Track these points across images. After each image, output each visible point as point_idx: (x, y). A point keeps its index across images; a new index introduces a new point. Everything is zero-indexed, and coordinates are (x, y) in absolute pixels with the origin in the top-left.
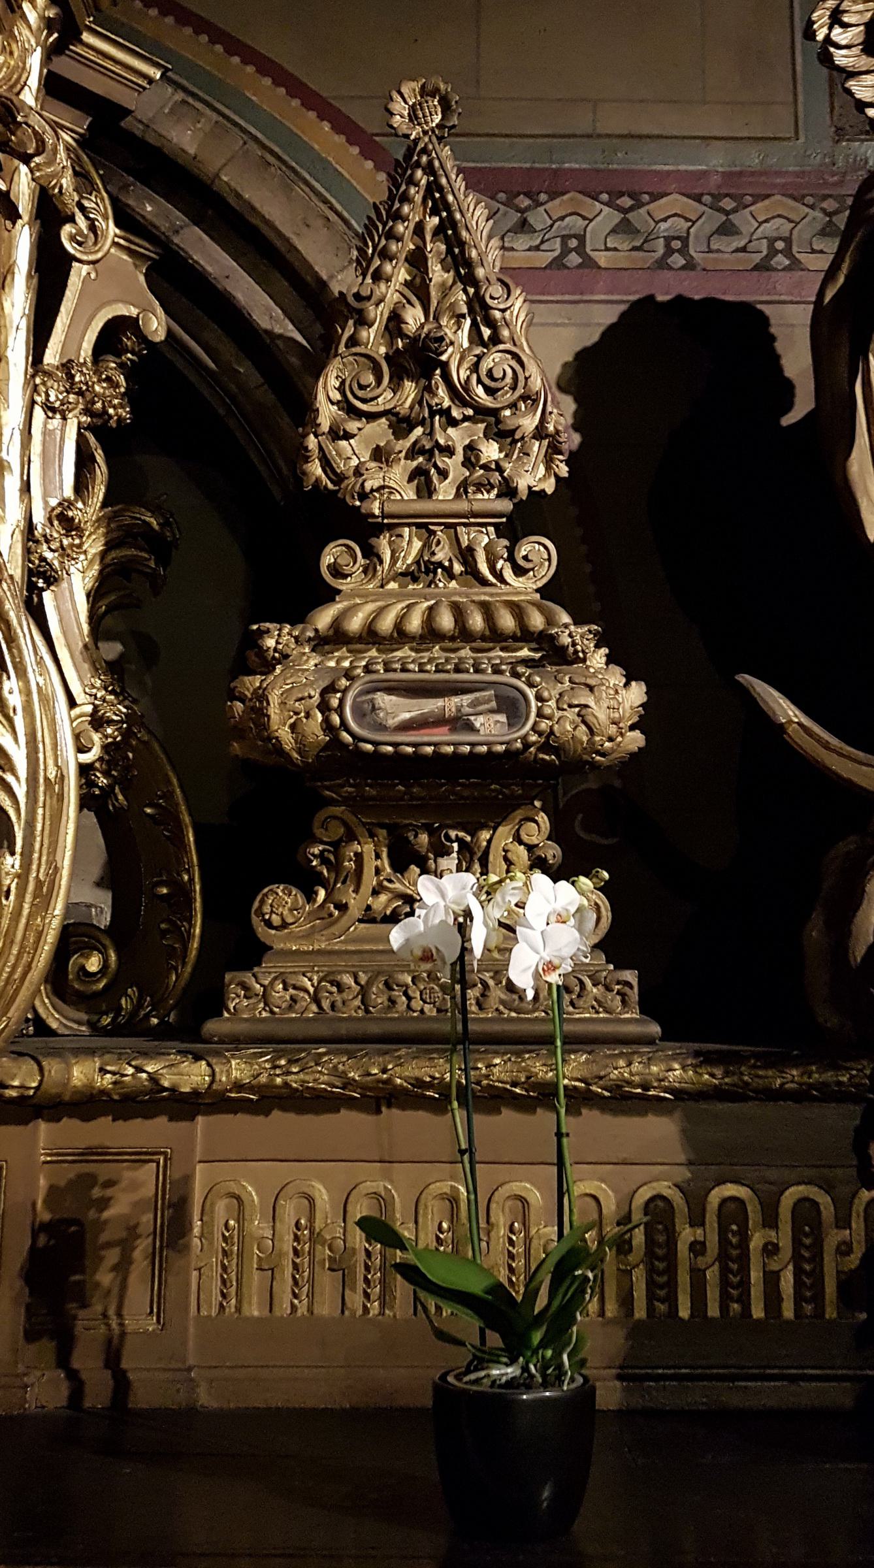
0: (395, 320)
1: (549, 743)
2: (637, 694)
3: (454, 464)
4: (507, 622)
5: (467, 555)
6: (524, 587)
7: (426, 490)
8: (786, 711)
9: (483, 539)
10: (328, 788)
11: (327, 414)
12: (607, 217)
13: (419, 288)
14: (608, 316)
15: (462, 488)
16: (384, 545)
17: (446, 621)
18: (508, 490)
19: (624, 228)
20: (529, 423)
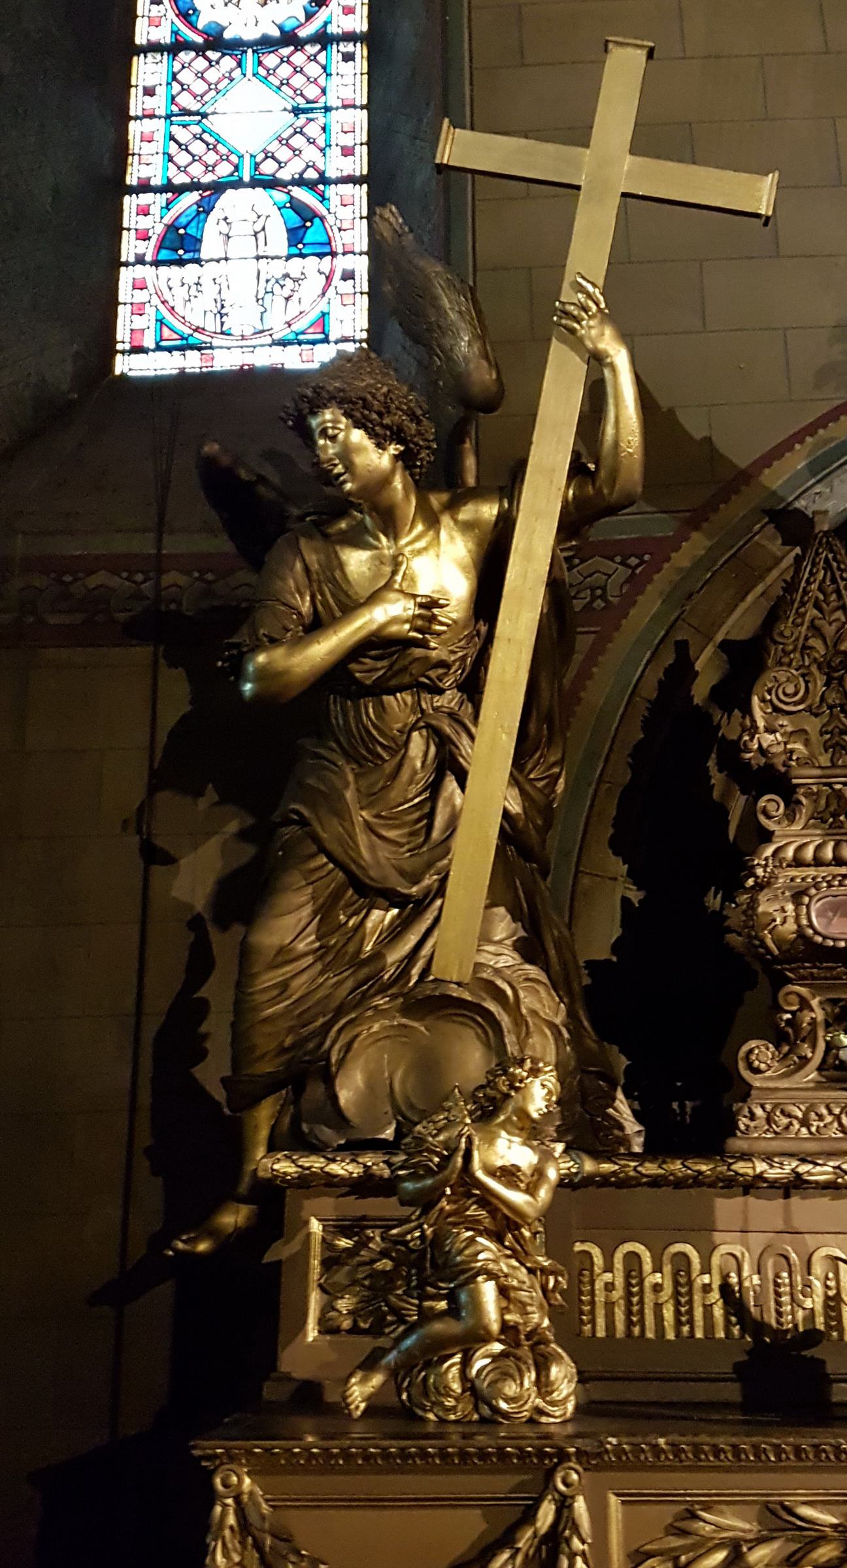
10: (790, 970)
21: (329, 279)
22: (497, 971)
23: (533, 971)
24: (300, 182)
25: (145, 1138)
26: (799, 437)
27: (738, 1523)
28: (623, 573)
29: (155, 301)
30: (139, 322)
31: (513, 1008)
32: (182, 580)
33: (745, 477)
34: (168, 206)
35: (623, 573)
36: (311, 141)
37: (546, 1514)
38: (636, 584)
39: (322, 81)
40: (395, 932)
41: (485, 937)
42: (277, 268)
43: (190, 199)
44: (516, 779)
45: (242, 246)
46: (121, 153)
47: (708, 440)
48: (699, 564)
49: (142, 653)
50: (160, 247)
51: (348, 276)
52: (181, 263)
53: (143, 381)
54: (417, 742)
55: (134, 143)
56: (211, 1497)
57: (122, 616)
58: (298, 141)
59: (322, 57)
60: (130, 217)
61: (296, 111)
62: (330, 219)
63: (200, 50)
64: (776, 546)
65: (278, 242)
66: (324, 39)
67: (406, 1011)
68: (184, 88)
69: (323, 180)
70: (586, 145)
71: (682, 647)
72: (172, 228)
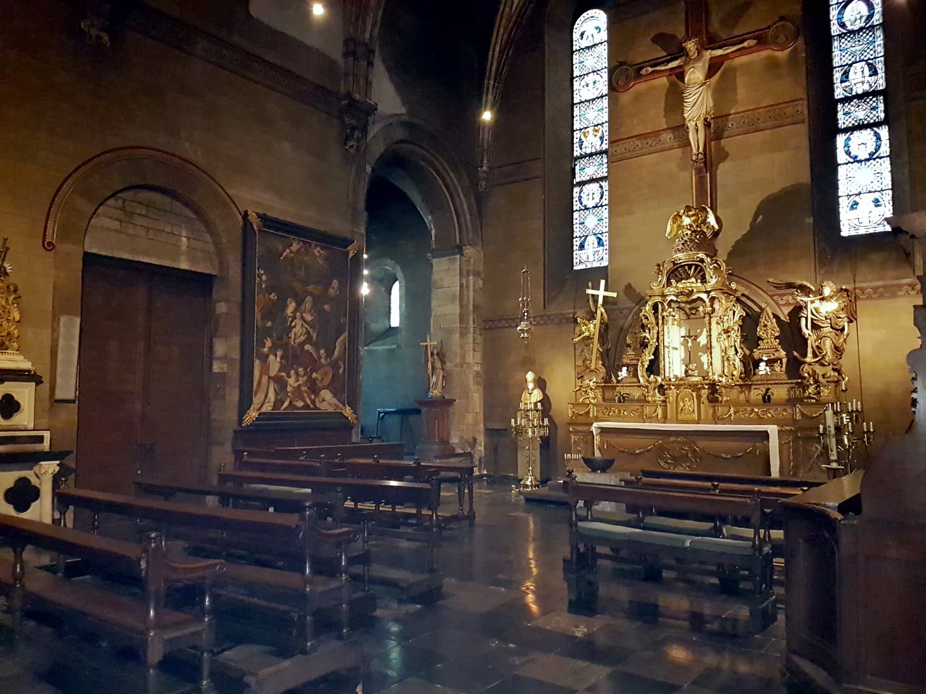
6: (776, 344)
9: (773, 340)
11: (758, 330)
12: (791, 298)
13: (766, 319)
42: (595, 250)
43: (583, 238)
45: (591, 246)
55: (575, 230)
60: (575, 243)
63: (583, 210)
66: (602, 206)
72: (581, 244)
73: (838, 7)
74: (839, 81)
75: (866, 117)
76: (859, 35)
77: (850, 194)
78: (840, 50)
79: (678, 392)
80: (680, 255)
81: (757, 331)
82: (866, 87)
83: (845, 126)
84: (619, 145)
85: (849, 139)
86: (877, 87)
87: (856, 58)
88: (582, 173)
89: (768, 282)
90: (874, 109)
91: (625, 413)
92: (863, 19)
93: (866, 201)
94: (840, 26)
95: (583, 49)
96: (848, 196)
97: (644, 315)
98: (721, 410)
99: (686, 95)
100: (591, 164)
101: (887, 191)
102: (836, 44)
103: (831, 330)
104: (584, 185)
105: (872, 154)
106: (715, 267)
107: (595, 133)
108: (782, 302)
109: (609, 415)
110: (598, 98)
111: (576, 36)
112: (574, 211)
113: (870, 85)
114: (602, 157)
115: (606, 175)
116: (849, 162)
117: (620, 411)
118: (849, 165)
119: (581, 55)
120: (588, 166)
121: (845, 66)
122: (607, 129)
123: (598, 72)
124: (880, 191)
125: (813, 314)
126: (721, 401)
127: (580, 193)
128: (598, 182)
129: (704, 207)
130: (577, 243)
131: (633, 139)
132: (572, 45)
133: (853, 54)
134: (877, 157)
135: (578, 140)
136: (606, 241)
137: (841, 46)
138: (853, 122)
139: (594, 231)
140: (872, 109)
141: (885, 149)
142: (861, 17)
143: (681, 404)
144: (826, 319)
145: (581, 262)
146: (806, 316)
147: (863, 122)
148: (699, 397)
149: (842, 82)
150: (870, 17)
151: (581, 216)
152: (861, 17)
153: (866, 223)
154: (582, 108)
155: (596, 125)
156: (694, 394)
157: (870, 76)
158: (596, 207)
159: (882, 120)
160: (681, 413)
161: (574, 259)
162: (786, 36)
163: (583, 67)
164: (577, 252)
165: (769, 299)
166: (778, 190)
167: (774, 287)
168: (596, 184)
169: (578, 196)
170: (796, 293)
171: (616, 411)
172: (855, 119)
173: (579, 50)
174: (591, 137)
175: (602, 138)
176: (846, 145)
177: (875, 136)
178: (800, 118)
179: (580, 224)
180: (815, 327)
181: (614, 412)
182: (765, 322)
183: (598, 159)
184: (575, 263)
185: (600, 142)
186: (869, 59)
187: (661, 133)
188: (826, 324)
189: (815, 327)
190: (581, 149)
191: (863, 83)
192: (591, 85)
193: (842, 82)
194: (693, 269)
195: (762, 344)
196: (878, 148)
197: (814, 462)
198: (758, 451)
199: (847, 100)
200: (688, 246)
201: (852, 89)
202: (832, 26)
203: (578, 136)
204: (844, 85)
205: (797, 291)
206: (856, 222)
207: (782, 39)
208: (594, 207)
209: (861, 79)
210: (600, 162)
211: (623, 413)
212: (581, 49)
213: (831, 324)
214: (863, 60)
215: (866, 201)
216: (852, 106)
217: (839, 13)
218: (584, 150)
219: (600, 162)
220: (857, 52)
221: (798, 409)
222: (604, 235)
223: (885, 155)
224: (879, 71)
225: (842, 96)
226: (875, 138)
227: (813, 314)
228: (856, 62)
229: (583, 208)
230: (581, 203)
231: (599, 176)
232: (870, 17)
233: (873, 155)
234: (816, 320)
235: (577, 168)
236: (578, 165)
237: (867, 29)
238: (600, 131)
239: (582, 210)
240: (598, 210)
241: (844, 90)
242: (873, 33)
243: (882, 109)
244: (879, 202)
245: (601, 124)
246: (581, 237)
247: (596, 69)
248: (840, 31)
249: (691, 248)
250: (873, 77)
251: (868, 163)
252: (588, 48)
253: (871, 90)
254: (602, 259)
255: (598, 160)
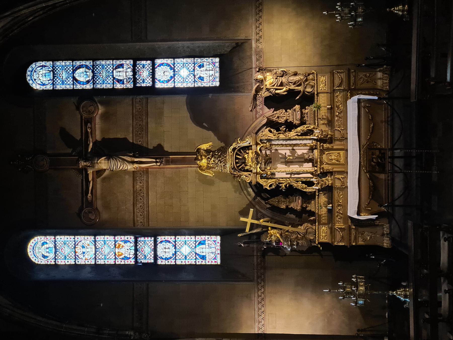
0: (276, 118)
1: (300, 110)
2: (297, 105)
3: (283, 115)
4: (292, 112)
5: (288, 114)
7: (285, 116)
8: (298, 97)
9: (287, 113)
11: (281, 122)
14: (265, 107)
15: (285, 115)
16: (288, 119)
17: (292, 115)
18: (285, 112)
19: (259, 106)
20: (281, 111)
21: (208, 240)
22: (304, 228)
23: (303, 225)
24: (195, 244)
25: (310, 255)
26: (247, 197)
27: (337, 218)
28: (259, 213)
29: (211, 260)
30: (214, 262)
31: (306, 227)
32: (259, 253)
33: (250, 202)
34: (198, 259)
35: (259, 213)
36: (190, 243)
37: (337, 228)
38: (261, 212)
39: (181, 241)
40: (300, 235)
41: (301, 229)
42: (207, 246)
43: (197, 256)
44: (288, 226)
45: (204, 250)
46: (191, 265)
47: (246, 205)
48: (259, 206)
49: (266, 257)
50: (204, 260)
51: (208, 238)
52: (206, 257)
53: (221, 261)
54: (286, 233)
55: (190, 263)
56: (336, 245)
57: (262, 259)
58: (190, 244)
59: (178, 242)
61: (186, 244)
62: (201, 240)
63: (176, 256)
64: (257, 199)
65: (204, 246)
67: (307, 234)
68: (182, 258)
69: (195, 241)
70: (247, 222)
71: (267, 208)
72: (201, 259)
73: (76, 84)
74: (122, 85)
75: (148, 70)
76: (96, 73)
77: (193, 80)
78: (103, 84)
79: (325, 164)
80: (228, 166)
81: (281, 123)
82: (129, 70)
83: (151, 82)
84: (137, 220)
85: (159, 81)
86: (130, 64)
87: (111, 75)
88: (148, 257)
89: (251, 111)
90: (144, 66)
91: (340, 201)
92: (87, 70)
93: (199, 72)
94: (88, 83)
95: (55, 256)
96: (194, 82)
97: (269, 187)
98: (337, 135)
99: (115, 167)
100: (143, 250)
101: (195, 61)
102: (99, 86)
103: (283, 77)
104: (157, 256)
105: (171, 68)
106: (239, 140)
107: (121, 247)
108: (261, 112)
109: (342, 214)
110: (95, 245)
111: (43, 262)
112: (176, 264)
113: (129, 68)
114: (140, 241)
115: (153, 238)
116: (174, 81)
117: (339, 205)
118: (175, 81)
119: (59, 258)
120: (144, 252)
121: (113, 82)
122: (119, 237)
123: (76, 244)
124: (195, 65)
125: (274, 86)
126: (332, 135)
127: (162, 259)
128: (157, 245)
129: (196, 150)
130: (200, 262)
131: (135, 210)
132: (50, 265)
133: (107, 77)
134: (174, 65)
135: (123, 261)
136: (202, 238)
137: (101, 83)
138: (150, 78)
139: (193, 248)
140: (144, 68)
141: (170, 61)
142: (86, 72)
143: (334, 161)
144: (277, 78)
145: (215, 258)
146: (275, 90)
147: (151, 72)
148: (328, 149)
149: (123, 83)
150: (87, 67)
151: (180, 258)
152: (86, 72)
153: (211, 73)
154: (99, 257)
155: (115, 245)
156: (326, 153)
157: (123, 68)
158: (175, 246)
159: (151, 62)
160: (340, 162)
161: (212, 263)
162: (90, 106)
163: (69, 256)
164: (207, 261)
165: (258, 120)
166: (188, 113)
167: (254, 109)
168: (158, 246)
169: (165, 261)
170: (259, 95)
171: (340, 208)
172: (148, 77)
173: (55, 259)
174: (123, 251)
175: (126, 242)
176: (163, 82)
177: (160, 66)
178: (144, 101)
179: (186, 259)
180: (282, 84)
181: (339, 210)
182: (276, 117)
183: (140, 245)
184: (215, 263)
185: (128, 244)
186: (113, 68)
187: (135, 189)
188: (281, 79)
189: (282, 84)
190: (130, 258)
191: (126, 72)
192: (84, 250)
193: (123, 83)
194: (238, 157)
195: (290, 120)
196: (168, 65)
197: (370, 79)
198: (367, 105)
199: (135, 81)
200: (223, 159)
201: (129, 78)
202: (87, 88)
203: (120, 260)
204: (125, 83)
205: (258, 95)
206: (211, 78)
207: (92, 108)
208: (175, 248)
209: (124, 73)
210: (143, 242)
211: (341, 202)
212: (55, 257)
213: (280, 77)
214: (113, 71)
215: (199, 72)
216: (139, 78)
217: (80, 84)
218: (131, 256)
219: (143, 242)
220: (107, 74)
221: (336, 89)
222: (197, 240)
223: (173, 61)
224: (122, 63)
225: (132, 84)
226: (162, 66)
227: (274, 86)
228: (113, 75)
229: (175, 256)
230: (171, 258)
231: (153, 244)
232: (87, 67)
233: (172, 68)
234: (277, 85)
235: (143, 261)
236: (141, 260)
237: (94, 68)
238: (120, 243)
239: (175, 257)
240: (178, 244)
241: (128, 83)
242: (97, 65)
243: (145, 62)
244: (201, 64)
245: (115, 242)
246: (196, 258)
247: (74, 246)
248: (91, 84)
249: (224, 157)
250: (124, 66)
251: (177, 70)
252: (55, 253)
253: (132, 68)
254: (215, 241)
255: (141, 244)
